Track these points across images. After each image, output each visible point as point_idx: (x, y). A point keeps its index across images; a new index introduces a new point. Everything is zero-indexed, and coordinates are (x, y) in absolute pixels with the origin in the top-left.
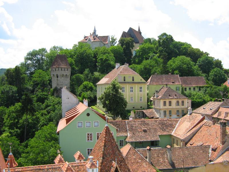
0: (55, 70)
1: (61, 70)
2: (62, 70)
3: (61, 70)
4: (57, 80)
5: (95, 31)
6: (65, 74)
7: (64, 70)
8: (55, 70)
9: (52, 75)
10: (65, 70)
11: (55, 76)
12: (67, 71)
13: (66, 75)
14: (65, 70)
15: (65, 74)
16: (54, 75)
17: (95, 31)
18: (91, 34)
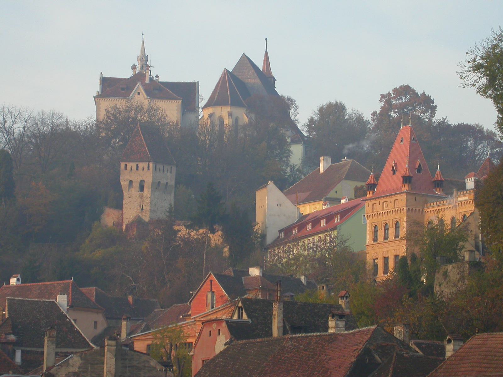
0: (137, 169)
1: (156, 170)
2: (158, 170)
3: (156, 170)
4: (141, 197)
5: (144, 59)
6: (163, 182)
7: (162, 171)
8: (137, 169)
9: (127, 183)
10: (163, 171)
11: (136, 185)
12: (169, 174)
13: (167, 183)
14: (163, 171)
15: (163, 182)
16: (131, 182)
17: (144, 59)
18: (134, 68)
